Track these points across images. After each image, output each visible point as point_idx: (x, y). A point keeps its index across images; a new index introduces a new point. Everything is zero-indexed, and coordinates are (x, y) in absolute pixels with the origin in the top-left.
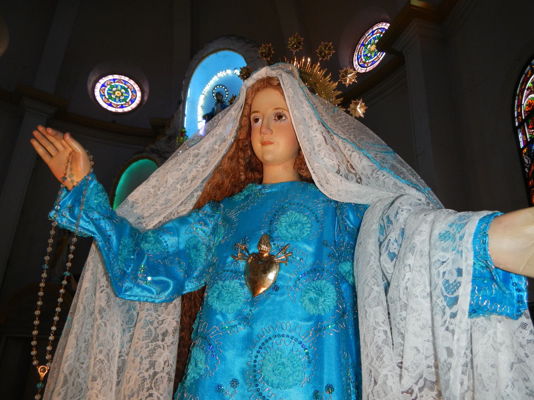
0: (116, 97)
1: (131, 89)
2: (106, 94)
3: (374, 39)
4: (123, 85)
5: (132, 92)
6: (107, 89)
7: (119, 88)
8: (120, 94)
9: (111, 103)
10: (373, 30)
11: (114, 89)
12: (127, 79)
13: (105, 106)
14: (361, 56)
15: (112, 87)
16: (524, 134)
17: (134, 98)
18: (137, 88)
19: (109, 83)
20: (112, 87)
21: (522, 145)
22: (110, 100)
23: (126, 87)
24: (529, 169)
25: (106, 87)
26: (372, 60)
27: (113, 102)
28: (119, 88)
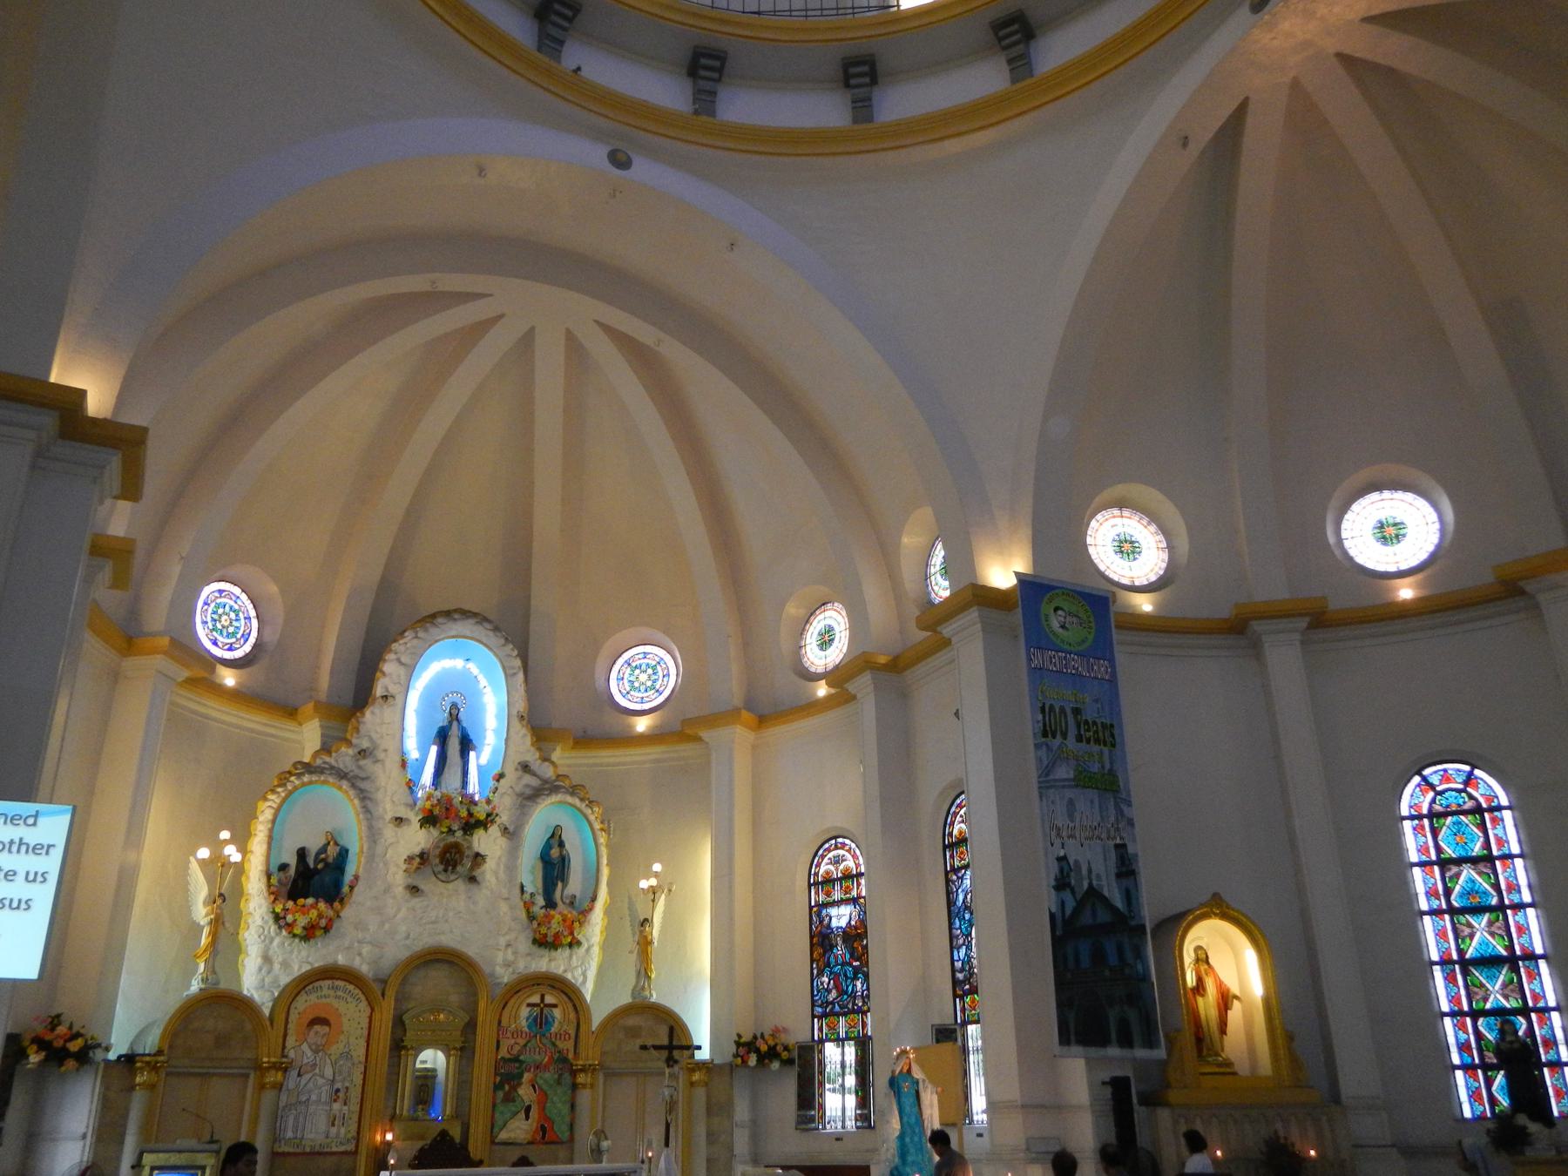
0: (223, 627)
1: (243, 613)
2: (209, 619)
3: (648, 665)
4: (232, 603)
5: (245, 618)
6: (210, 611)
7: (227, 608)
8: (228, 622)
9: (216, 639)
10: (646, 651)
11: (220, 611)
12: (237, 590)
13: (208, 645)
14: (623, 679)
15: (218, 606)
16: (817, 893)
17: (248, 631)
18: (253, 613)
19: (213, 598)
20: (218, 606)
21: (813, 904)
22: (214, 633)
23: (236, 607)
24: (817, 928)
25: (209, 605)
26: (640, 695)
27: (219, 638)
28: (227, 608)
